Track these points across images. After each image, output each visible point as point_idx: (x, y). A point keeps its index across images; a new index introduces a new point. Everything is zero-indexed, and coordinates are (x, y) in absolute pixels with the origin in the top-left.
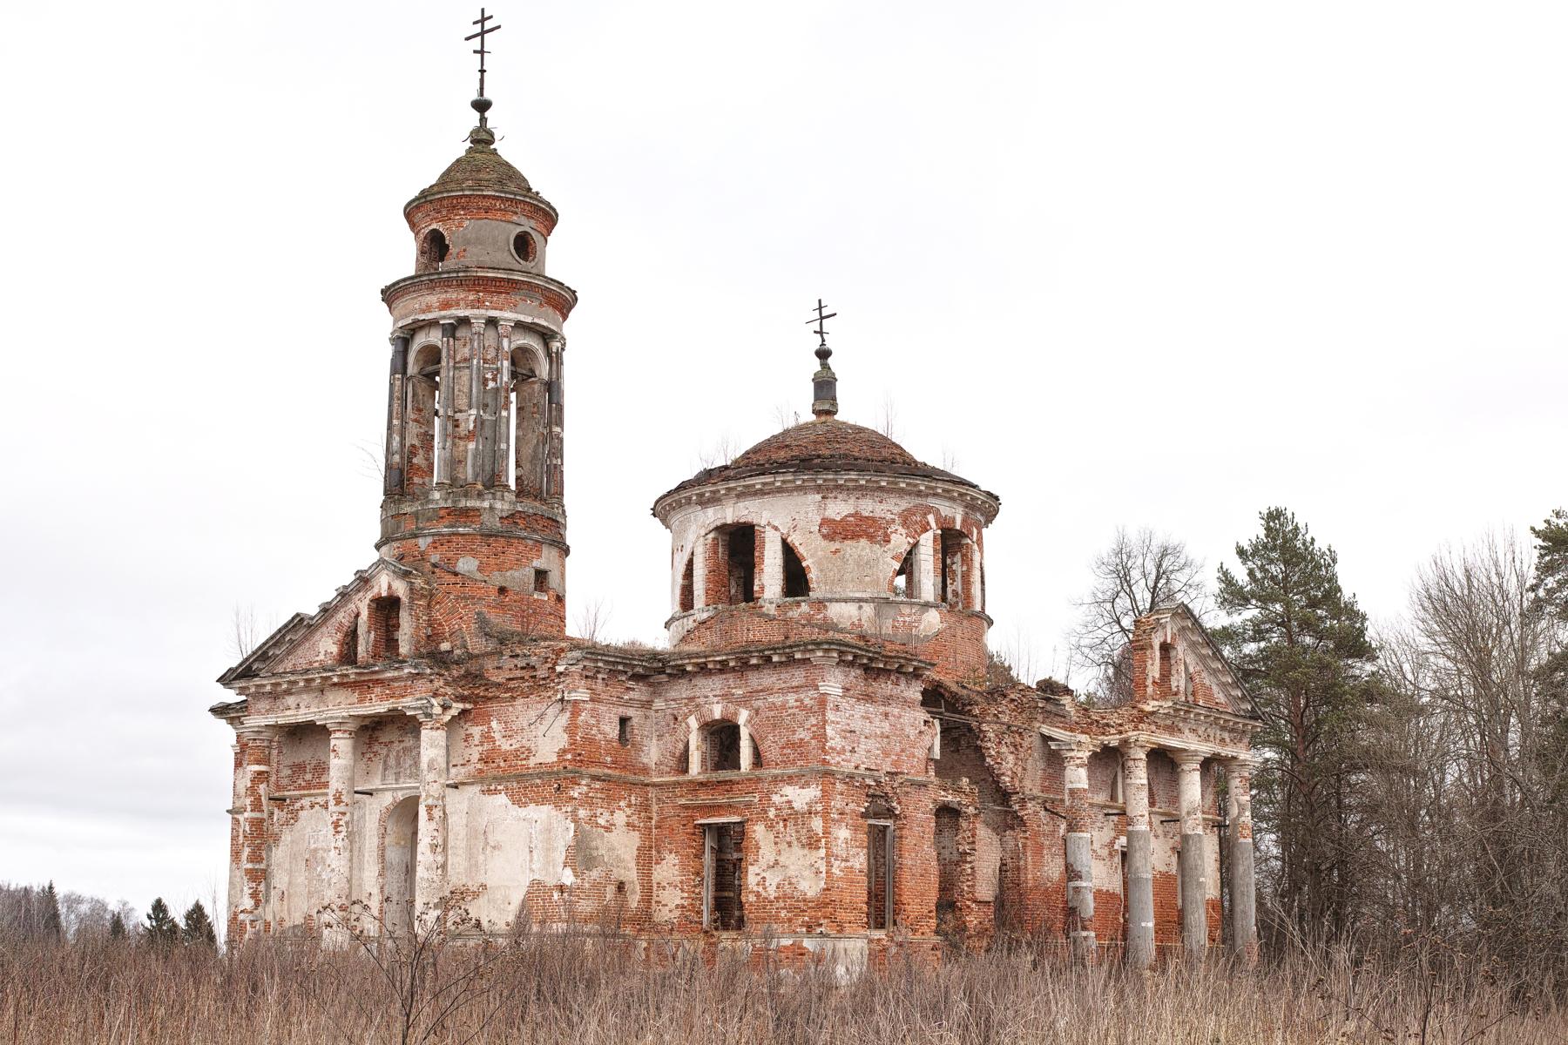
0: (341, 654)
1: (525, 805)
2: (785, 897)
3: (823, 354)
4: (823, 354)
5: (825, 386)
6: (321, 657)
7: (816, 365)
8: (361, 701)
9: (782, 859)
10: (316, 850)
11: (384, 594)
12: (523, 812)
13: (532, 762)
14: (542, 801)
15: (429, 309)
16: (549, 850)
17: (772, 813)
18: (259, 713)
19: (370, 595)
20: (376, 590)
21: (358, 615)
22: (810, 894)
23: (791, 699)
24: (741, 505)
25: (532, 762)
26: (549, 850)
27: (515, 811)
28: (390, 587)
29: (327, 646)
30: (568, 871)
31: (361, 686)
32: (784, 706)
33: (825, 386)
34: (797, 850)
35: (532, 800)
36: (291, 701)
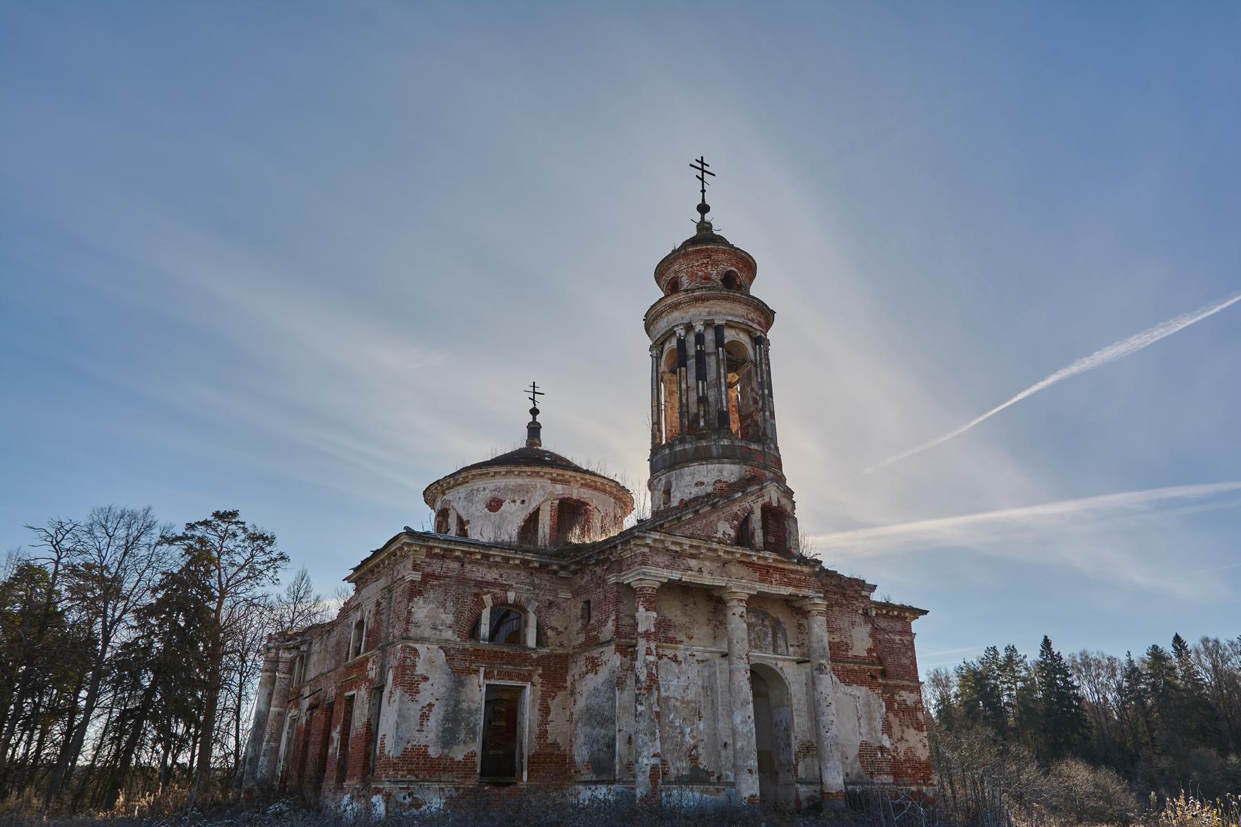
0: (737, 537)
1: (849, 684)
2: (909, 760)
3: (534, 412)
4: (534, 412)
5: (534, 430)
6: (720, 535)
7: (530, 418)
8: (761, 581)
9: (905, 736)
10: (668, 698)
11: (775, 504)
12: (849, 690)
13: (850, 654)
14: (862, 684)
15: (752, 321)
16: (871, 719)
17: (896, 706)
18: (657, 565)
19: (761, 502)
20: (767, 499)
21: (751, 512)
22: (923, 758)
23: (897, 638)
24: (582, 490)
25: (850, 654)
26: (871, 719)
27: (843, 688)
28: (779, 501)
29: (725, 529)
30: (886, 737)
31: (764, 572)
32: (893, 641)
33: (534, 430)
34: (912, 730)
35: (853, 682)
36: (693, 563)
